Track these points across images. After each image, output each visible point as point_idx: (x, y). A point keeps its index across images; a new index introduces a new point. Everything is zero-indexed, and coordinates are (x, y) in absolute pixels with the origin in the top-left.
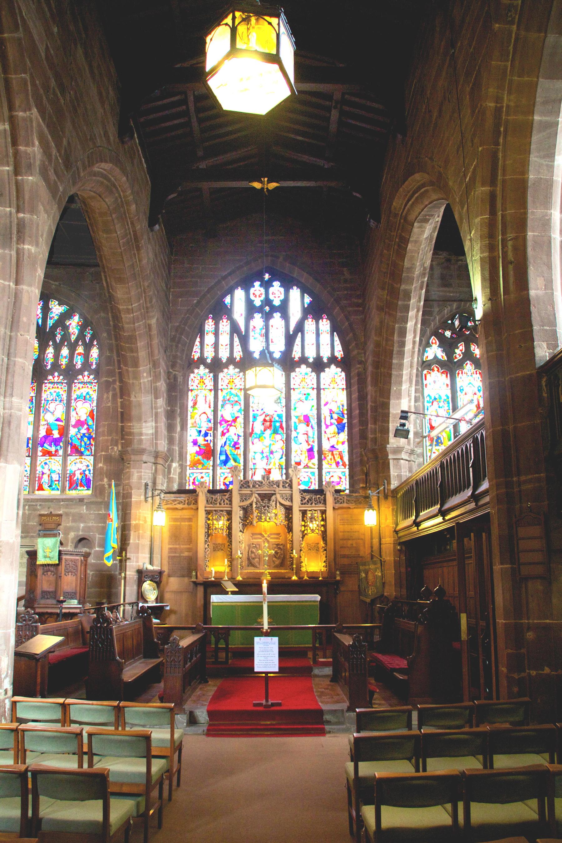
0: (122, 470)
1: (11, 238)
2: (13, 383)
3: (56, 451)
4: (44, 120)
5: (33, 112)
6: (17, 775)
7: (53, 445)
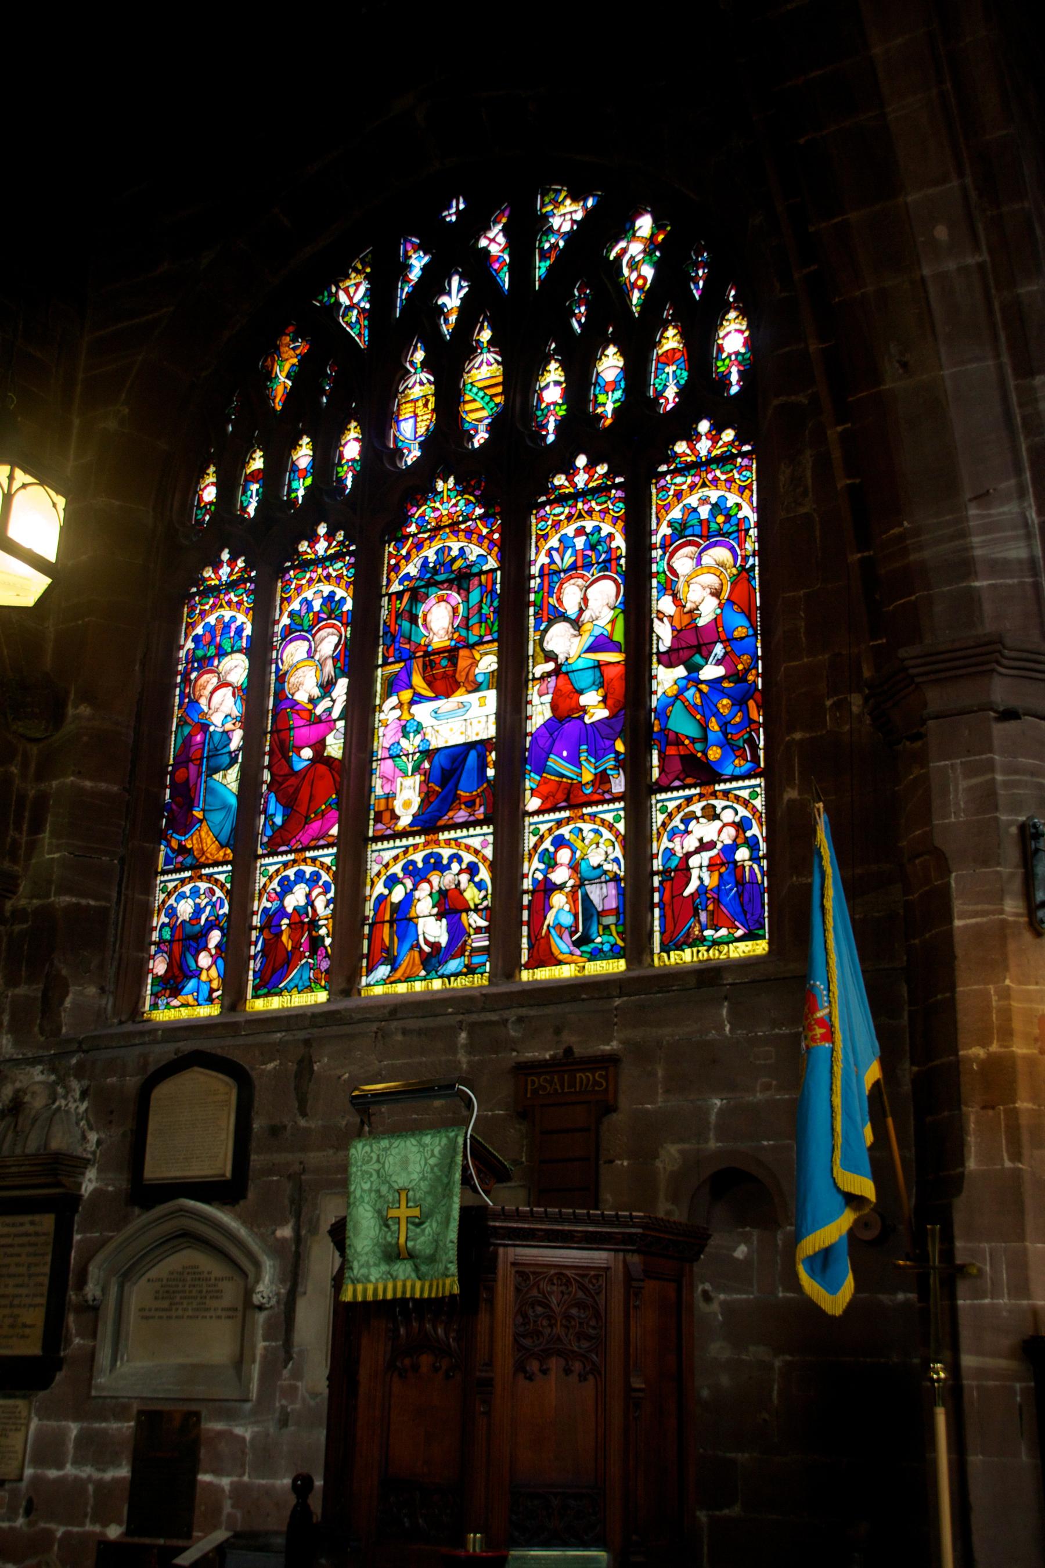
3: (602, 779)
7: (584, 756)
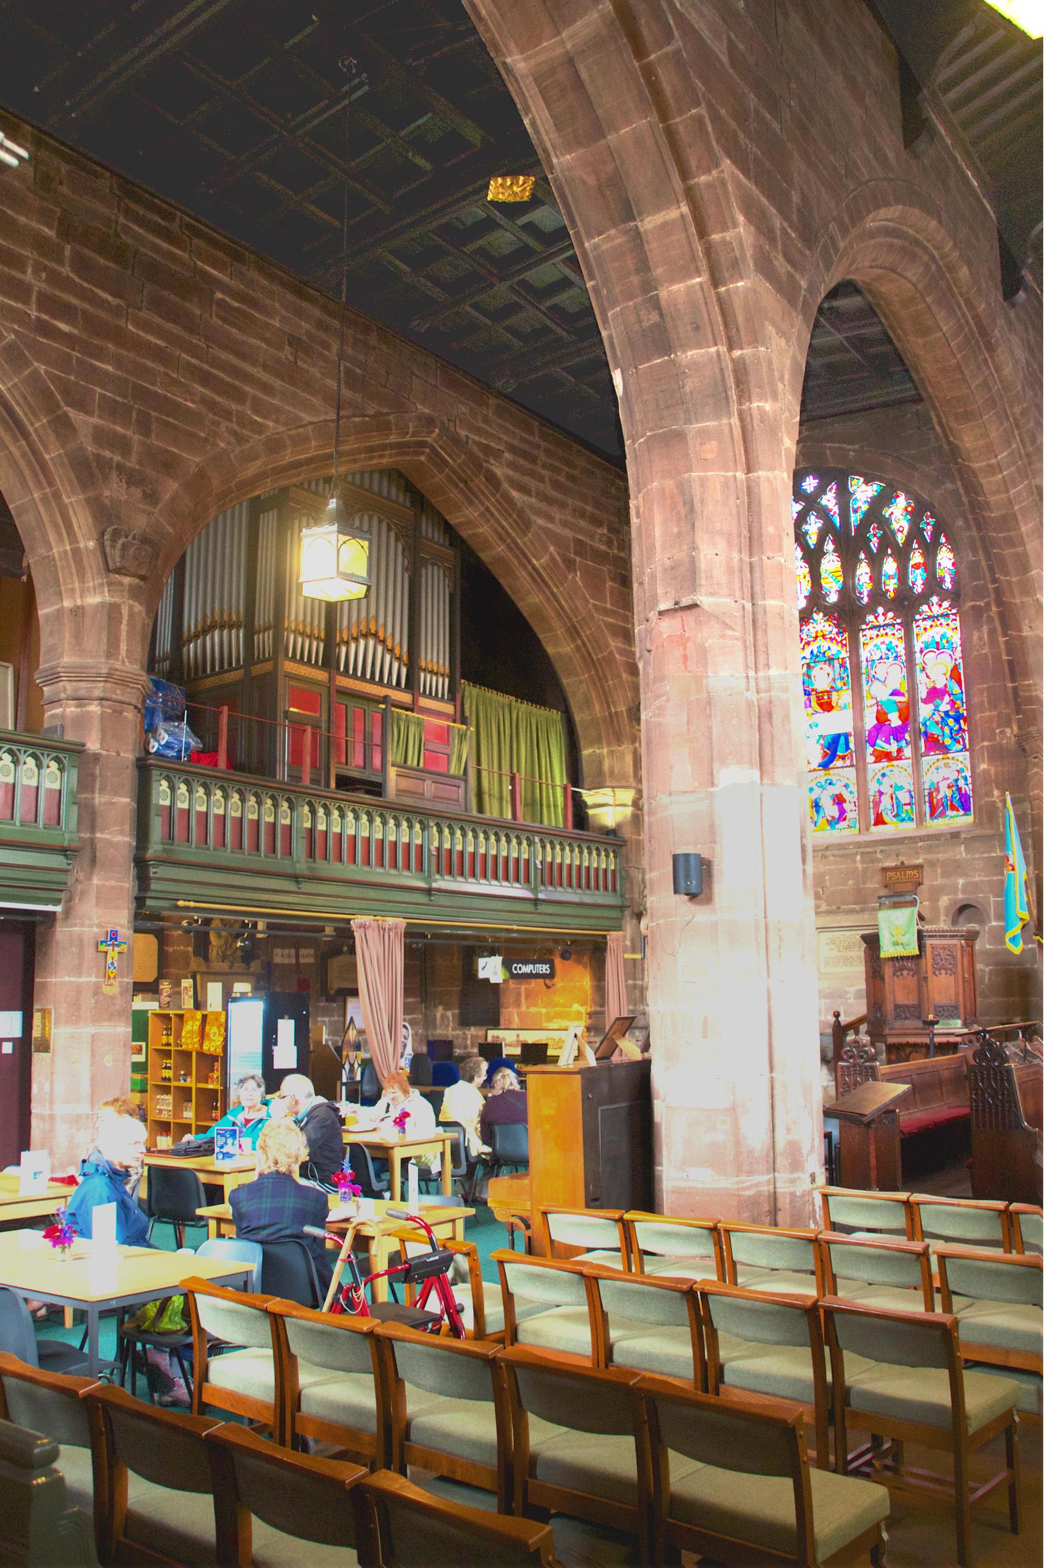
0: (1026, 770)
1: (727, 398)
2: (766, 645)
3: (900, 750)
4: (746, 172)
5: (723, 167)
6: (799, 1312)
7: (892, 741)
